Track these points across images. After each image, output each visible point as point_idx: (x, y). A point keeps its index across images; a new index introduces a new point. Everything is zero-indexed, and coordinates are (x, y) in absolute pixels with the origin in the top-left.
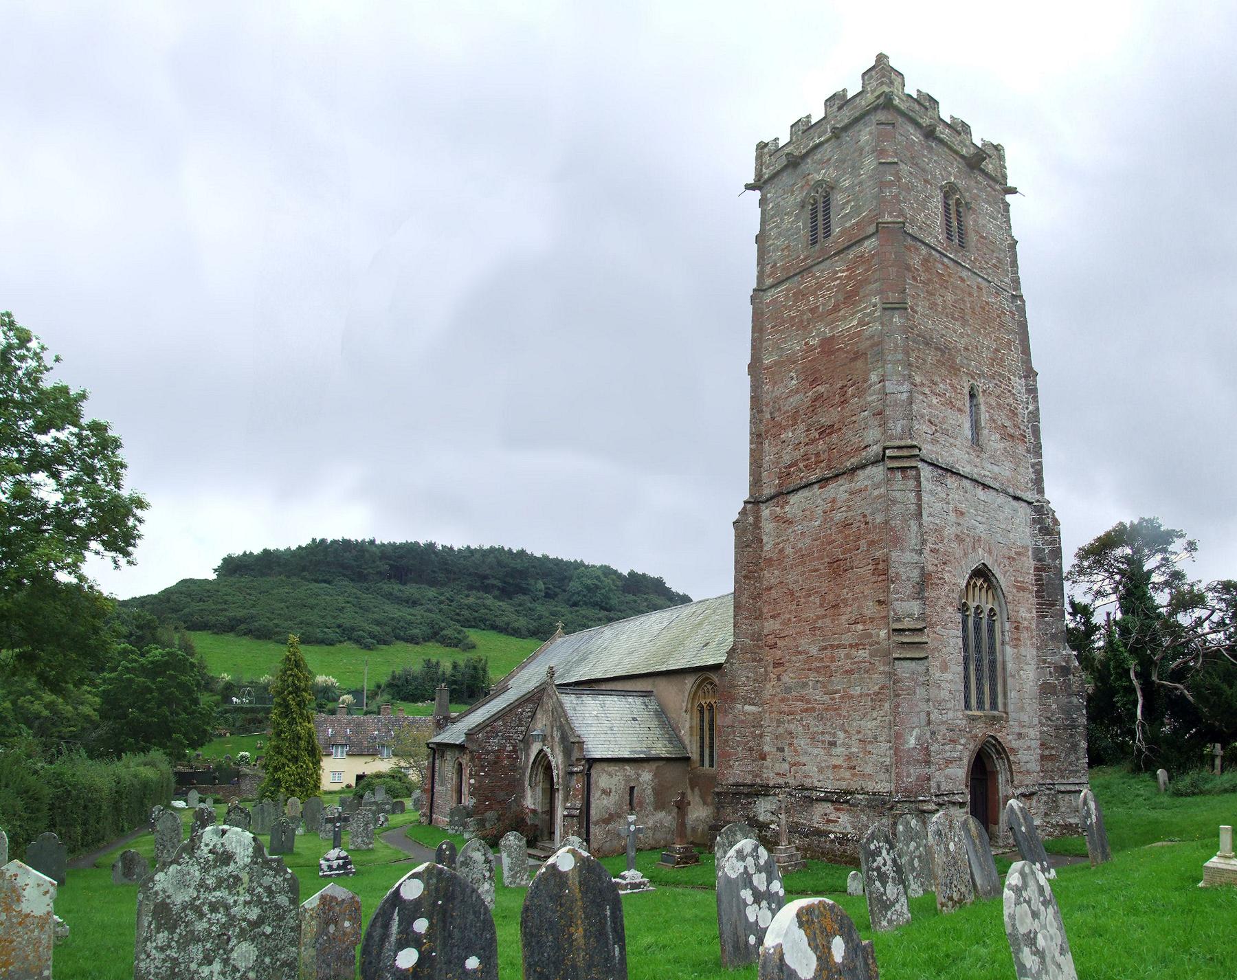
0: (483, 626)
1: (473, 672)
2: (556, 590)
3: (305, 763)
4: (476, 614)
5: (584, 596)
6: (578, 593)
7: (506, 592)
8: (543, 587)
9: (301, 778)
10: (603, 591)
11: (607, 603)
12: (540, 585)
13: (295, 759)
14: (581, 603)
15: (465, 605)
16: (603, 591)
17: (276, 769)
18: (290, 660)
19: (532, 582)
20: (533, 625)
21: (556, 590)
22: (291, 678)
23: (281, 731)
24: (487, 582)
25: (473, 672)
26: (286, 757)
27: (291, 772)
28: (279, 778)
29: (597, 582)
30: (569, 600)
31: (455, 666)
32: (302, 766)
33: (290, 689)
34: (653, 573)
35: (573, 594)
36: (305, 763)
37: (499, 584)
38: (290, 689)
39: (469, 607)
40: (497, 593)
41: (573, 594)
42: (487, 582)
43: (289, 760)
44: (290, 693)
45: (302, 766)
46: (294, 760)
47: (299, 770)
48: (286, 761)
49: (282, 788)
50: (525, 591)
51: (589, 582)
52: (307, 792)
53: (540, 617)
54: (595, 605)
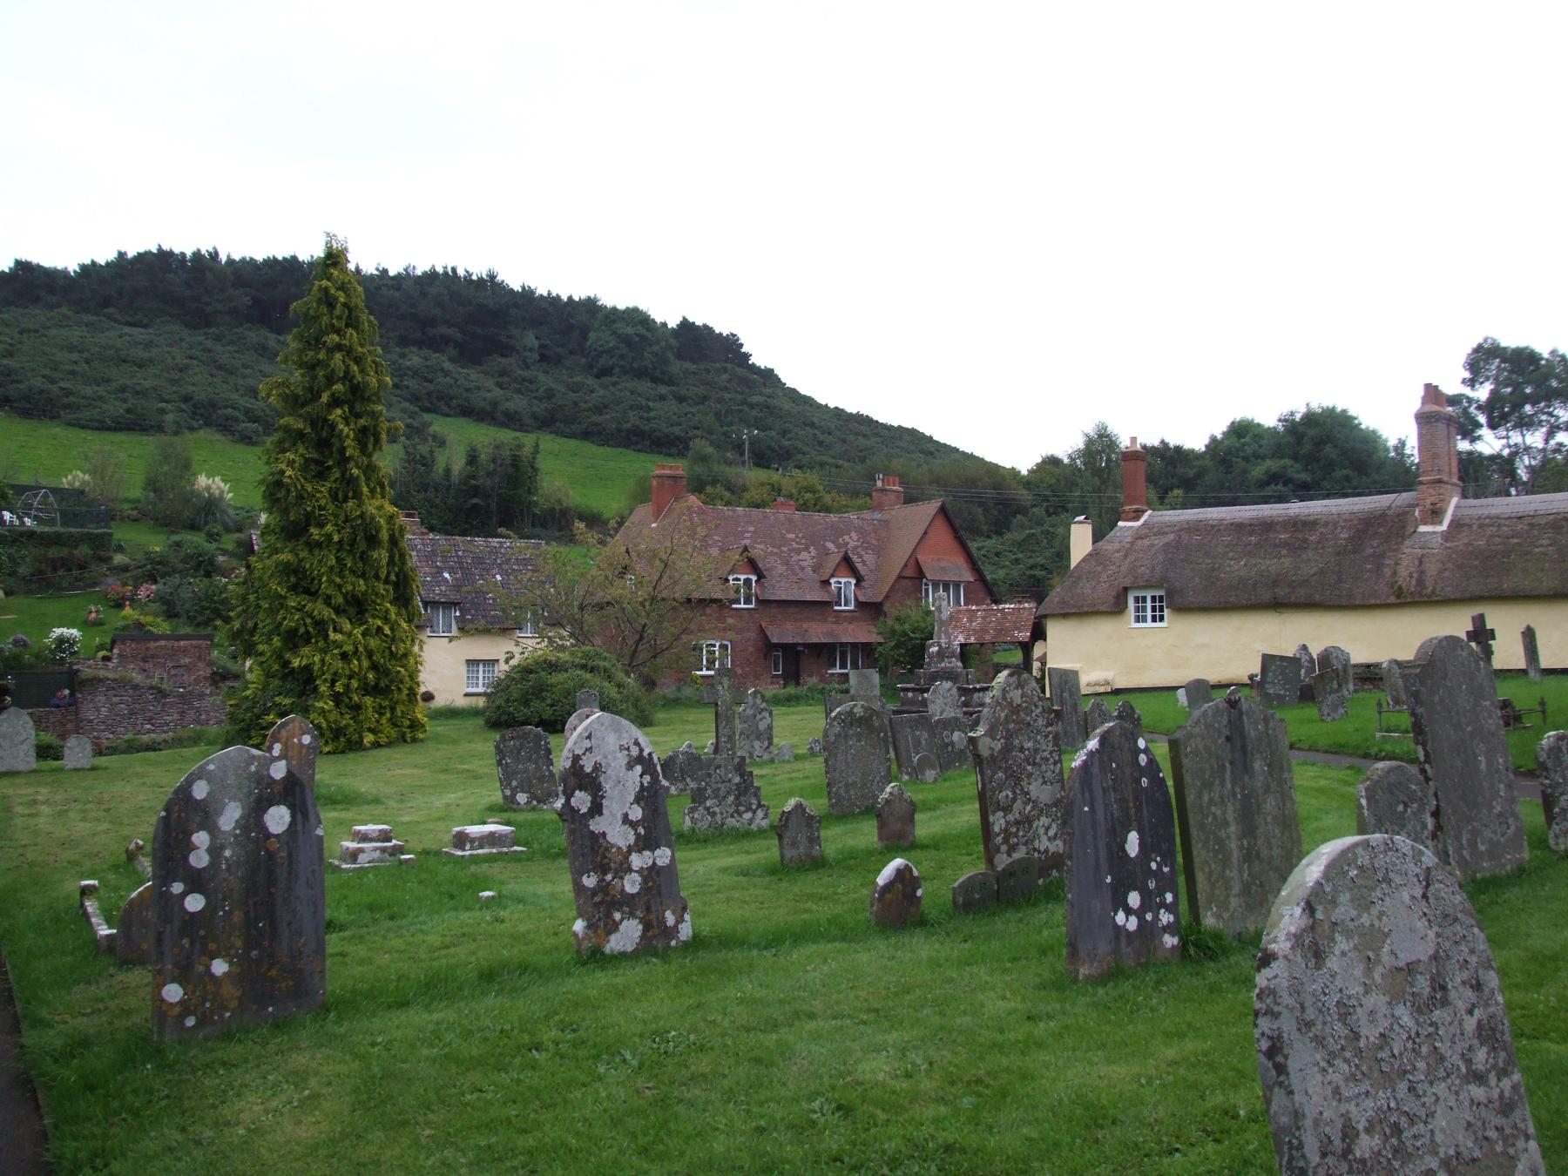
0: (446, 409)
1: (511, 470)
2: (559, 350)
3: (386, 619)
4: (431, 387)
5: (622, 357)
6: (609, 352)
7: (470, 354)
8: (536, 343)
9: (374, 667)
10: (656, 348)
11: (663, 373)
12: (530, 339)
13: (357, 607)
14: (617, 370)
15: (408, 368)
16: (656, 348)
17: (294, 640)
18: (331, 305)
19: (515, 332)
20: (540, 408)
21: (559, 350)
22: (338, 356)
23: (309, 519)
24: (431, 331)
25: (511, 470)
26: (327, 601)
27: (349, 648)
28: (307, 669)
29: (644, 332)
30: (591, 367)
31: (472, 459)
32: (379, 629)
33: (338, 387)
34: (722, 327)
35: (600, 354)
36: (386, 619)
37: (459, 336)
38: (338, 387)
39: (416, 374)
40: (453, 352)
41: (600, 354)
42: (431, 331)
43: (338, 611)
44: (336, 402)
45: (379, 629)
46: (352, 611)
47: (373, 643)
48: (327, 613)
49: (321, 697)
50: (505, 350)
51: (630, 330)
52: (393, 709)
53: (550, 395)
54: (641, 374)
